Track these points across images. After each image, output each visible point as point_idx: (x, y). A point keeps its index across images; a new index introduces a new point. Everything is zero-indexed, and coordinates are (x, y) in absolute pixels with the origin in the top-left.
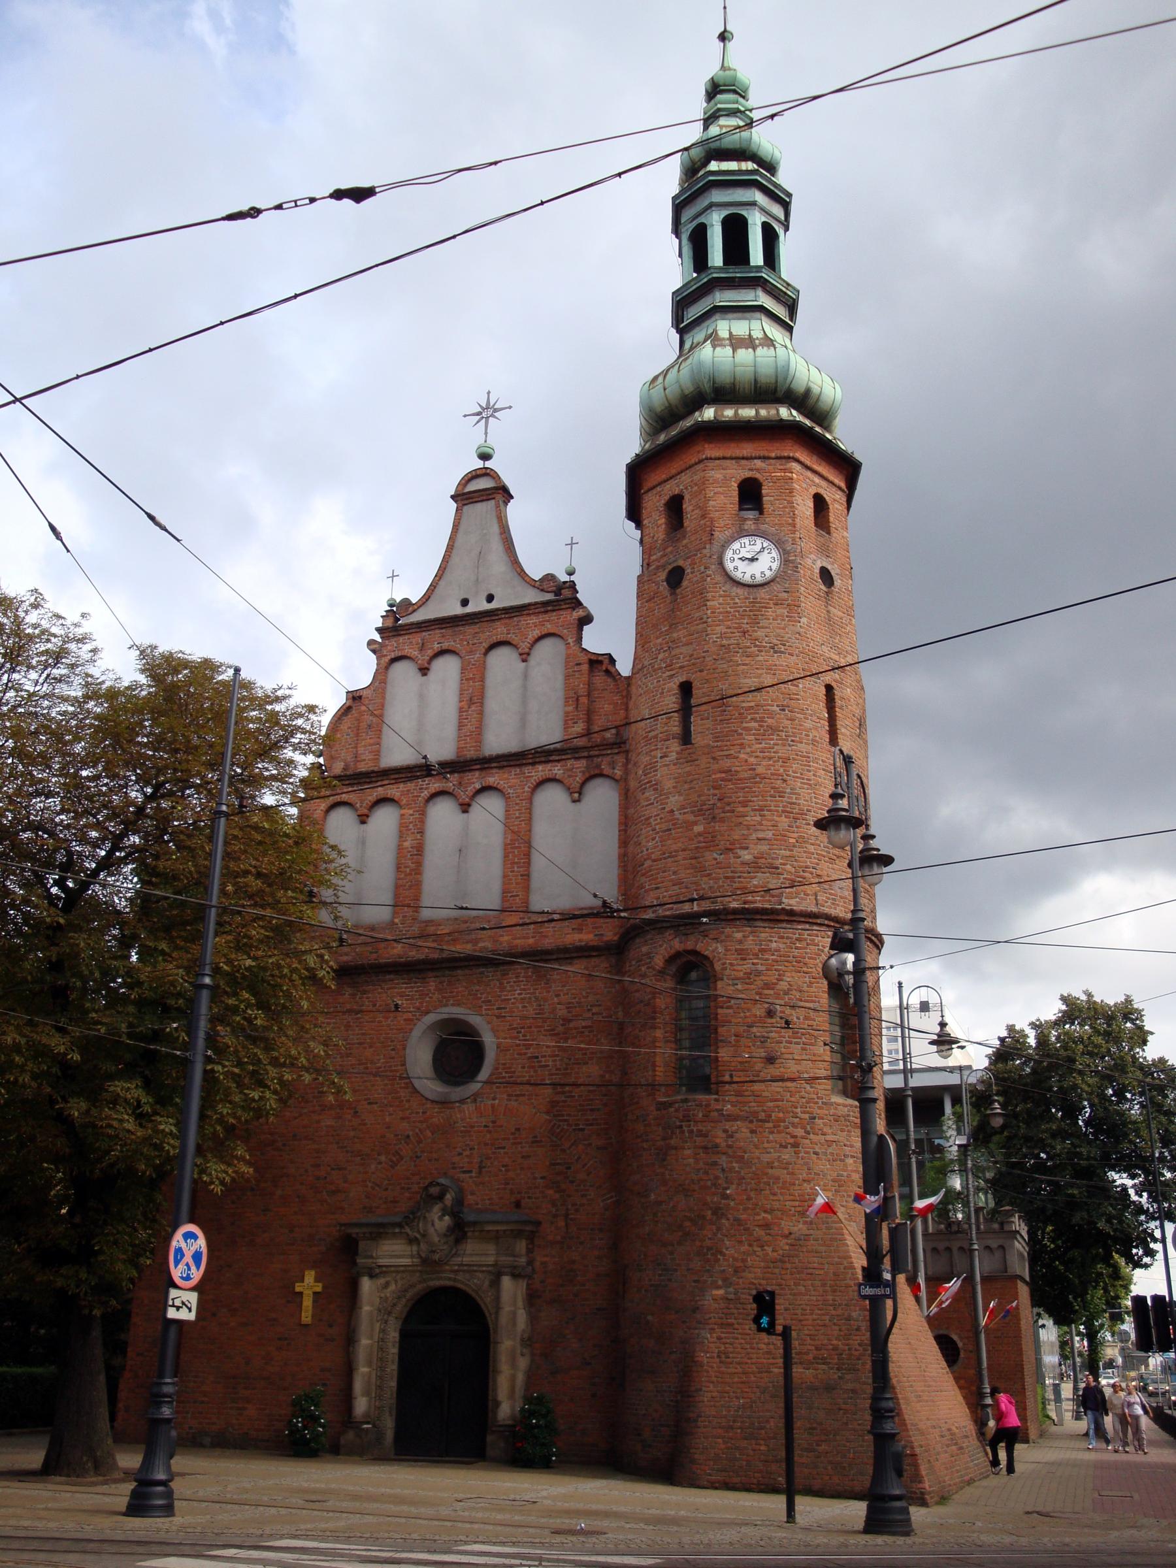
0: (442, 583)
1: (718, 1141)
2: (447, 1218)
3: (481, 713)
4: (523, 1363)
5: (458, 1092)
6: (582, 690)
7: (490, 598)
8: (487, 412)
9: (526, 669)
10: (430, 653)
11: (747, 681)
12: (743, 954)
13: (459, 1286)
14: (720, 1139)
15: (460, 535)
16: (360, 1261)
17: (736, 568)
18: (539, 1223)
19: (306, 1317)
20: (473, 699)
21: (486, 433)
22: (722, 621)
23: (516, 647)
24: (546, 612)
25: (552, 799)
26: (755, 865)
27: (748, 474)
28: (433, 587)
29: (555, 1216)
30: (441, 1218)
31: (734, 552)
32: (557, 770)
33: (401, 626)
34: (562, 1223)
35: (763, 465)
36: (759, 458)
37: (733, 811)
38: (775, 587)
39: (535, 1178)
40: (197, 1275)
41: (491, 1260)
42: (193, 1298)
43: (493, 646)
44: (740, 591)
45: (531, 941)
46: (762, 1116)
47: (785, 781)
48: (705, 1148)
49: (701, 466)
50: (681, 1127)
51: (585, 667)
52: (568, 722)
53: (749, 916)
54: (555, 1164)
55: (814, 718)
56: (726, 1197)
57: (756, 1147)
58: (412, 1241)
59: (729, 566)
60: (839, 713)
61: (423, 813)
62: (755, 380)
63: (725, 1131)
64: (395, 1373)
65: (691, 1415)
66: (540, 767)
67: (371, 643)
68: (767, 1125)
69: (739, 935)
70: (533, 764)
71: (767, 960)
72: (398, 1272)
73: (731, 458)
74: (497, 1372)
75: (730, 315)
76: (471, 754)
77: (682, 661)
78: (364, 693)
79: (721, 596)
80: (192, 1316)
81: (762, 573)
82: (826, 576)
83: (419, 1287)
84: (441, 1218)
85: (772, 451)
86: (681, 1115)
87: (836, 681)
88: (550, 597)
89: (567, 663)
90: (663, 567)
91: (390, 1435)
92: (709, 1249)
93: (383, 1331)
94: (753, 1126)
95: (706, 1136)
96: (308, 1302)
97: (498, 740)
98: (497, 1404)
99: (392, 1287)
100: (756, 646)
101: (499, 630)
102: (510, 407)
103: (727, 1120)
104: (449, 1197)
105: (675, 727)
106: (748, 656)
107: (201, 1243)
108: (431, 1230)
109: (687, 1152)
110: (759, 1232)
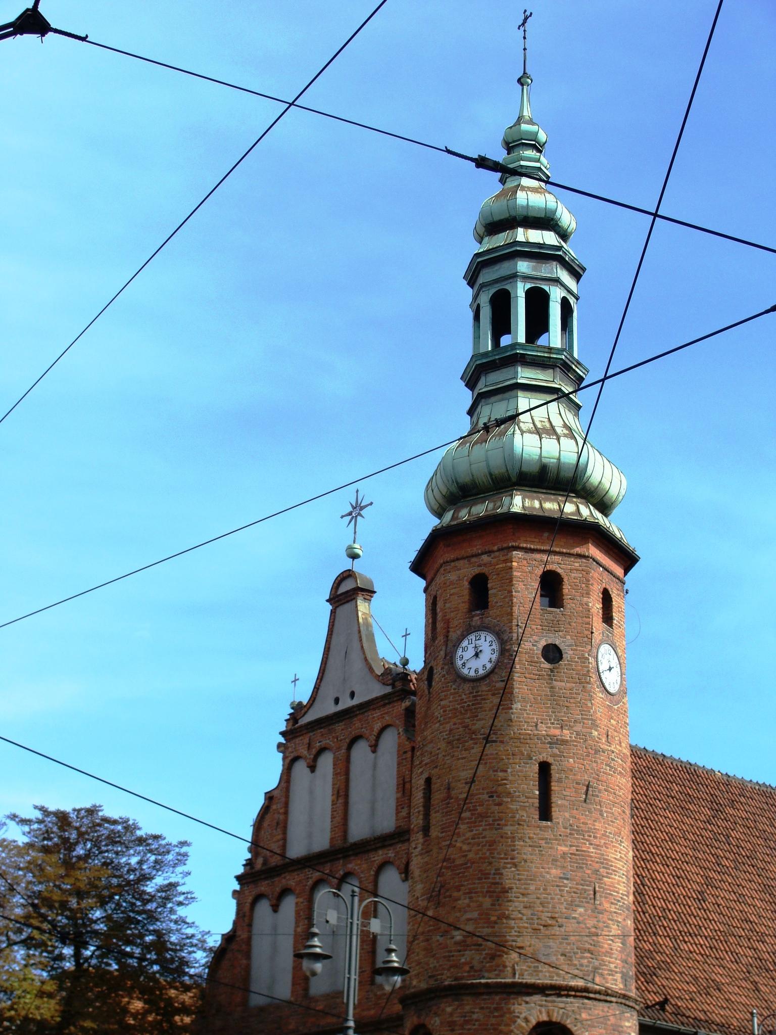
0: (323, 684)
3: (346, 804)
7: (352, 695)
8: (356, 511)
9: (375, 758)
10: (314, 751)
11: (465, 773)
15: (334, 636)
21: (355, 533)
22: (450, 718)
24: (384, 705)
26: (463, 945)
27: (477, 570)
28: (317, 689)
32: (391, 854)
33: (301, 726)
35: (489, 559)
36: (486, 553)
37: (450, 896)
38: (495, 678)
44: (467, 686)
45: (372, 1012)
47: (490, 863)
49: (442, 569)
51: (409, 754)
53: (458, 991)
55: (523, 799)
60: (554, 786)
61: (310, 901)
62: (491, 474)
66: (380, 852)
67: (279, 745)
69: (449, 1009)
70: (376, 849)
71: (469, 1029)
73: (463, 558)
75: (493, 399)
76: (339, 843)
77: (426, 760)
78: (275, 793)
79: (451, 694)
81: (484, 666)
82: (553, 654)
85: (494, 545)
87: (554, 756)
88: (389, 689)
89: (398, 751)
97: (359, 830)
100: (472, 739)
101: (357, 726)
102: (371, 504)
106: (466, 750)
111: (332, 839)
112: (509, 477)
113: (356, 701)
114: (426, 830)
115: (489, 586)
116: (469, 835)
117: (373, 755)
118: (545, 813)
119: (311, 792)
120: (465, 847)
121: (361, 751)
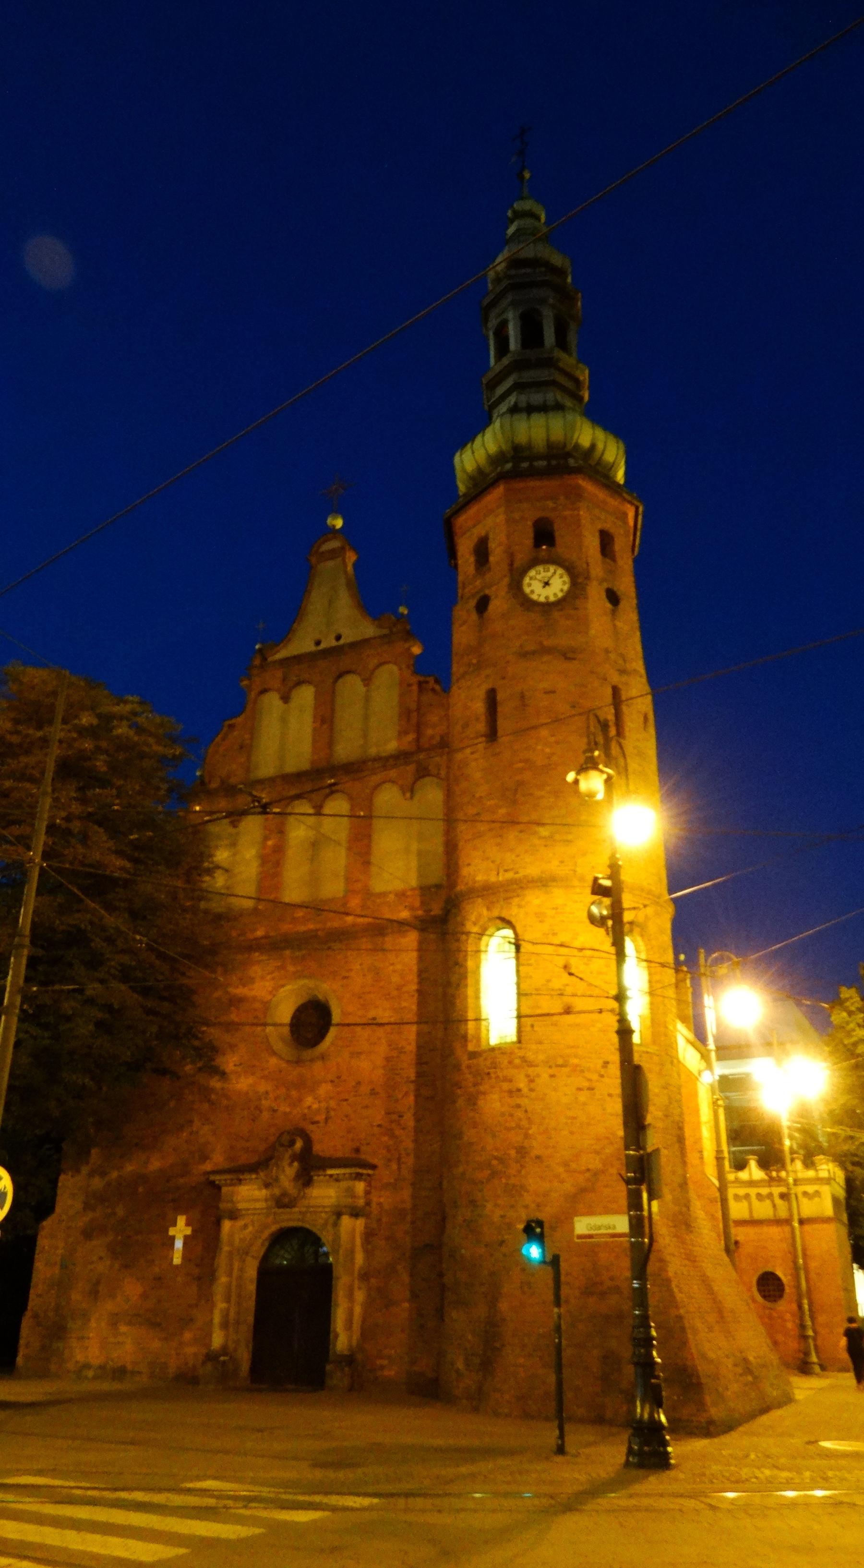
1: (522, 1085)
2: (296, 1164)
3: (331, 729)
4: (360, 1296)
5: (308, 1054)
6: (413, 706)
7: (338, 638)
9: (368, 691)
12: (541, 917)
13: (307, 1226)
14: (522, 1084)
16: (223, 1206)
17: (532, 592)
18: (374, 1167)
19: (177, 1260)
20: (326, 719)
23: (360, 674)
25: (388, 797)
29: (390, 1160)
30: (290, 1164)
31: (531, 578)
32: (393, 773)
34: (394, 1166)
39: (372, 1126)
41: (333, 1201)
43: (340, 676)
46: (560, 1061)
48: (510, 1092)
50: (489, 1074)
51: (415, 688)
52: (402, 733)
54: (389, 1114)
56: (527, 1136)
57: (555, 1090)
58: (267, 1185)
59: (527, 590)
63: (528, 1076)
64: (253, 1309)
65: (497, 1345)
68: (565, 1070)
69: (537, 902)
72: (254, 1214)
74: (337, 1305)
83: (274, 1228)
84: (290, 1164)
86: (488, 1063)
88: (385, 631)
90: (473, 596)
91: (245, 1367)
92: (514, 1186)
93: (241, 1270)
94: (552, 1071)
95: (511, 1081)
96: (179, 1244)
98: (337, 1336)
99: (250, 1228)
103: (528, 1066)
104: (299, 1144)
105: (482, 727)
108: (282, 1177)
109: (496, 1097)
110: (561, 1170)
111: (313, 762)
112: (565, 445)
113: (342, 642)
114: (492, 734)
115: (556, 527)
116: (553, 739)
117: (364, 689)
118: (620, 733)
119: (284, 720)
120: (548, 750)
121: (352, 685)
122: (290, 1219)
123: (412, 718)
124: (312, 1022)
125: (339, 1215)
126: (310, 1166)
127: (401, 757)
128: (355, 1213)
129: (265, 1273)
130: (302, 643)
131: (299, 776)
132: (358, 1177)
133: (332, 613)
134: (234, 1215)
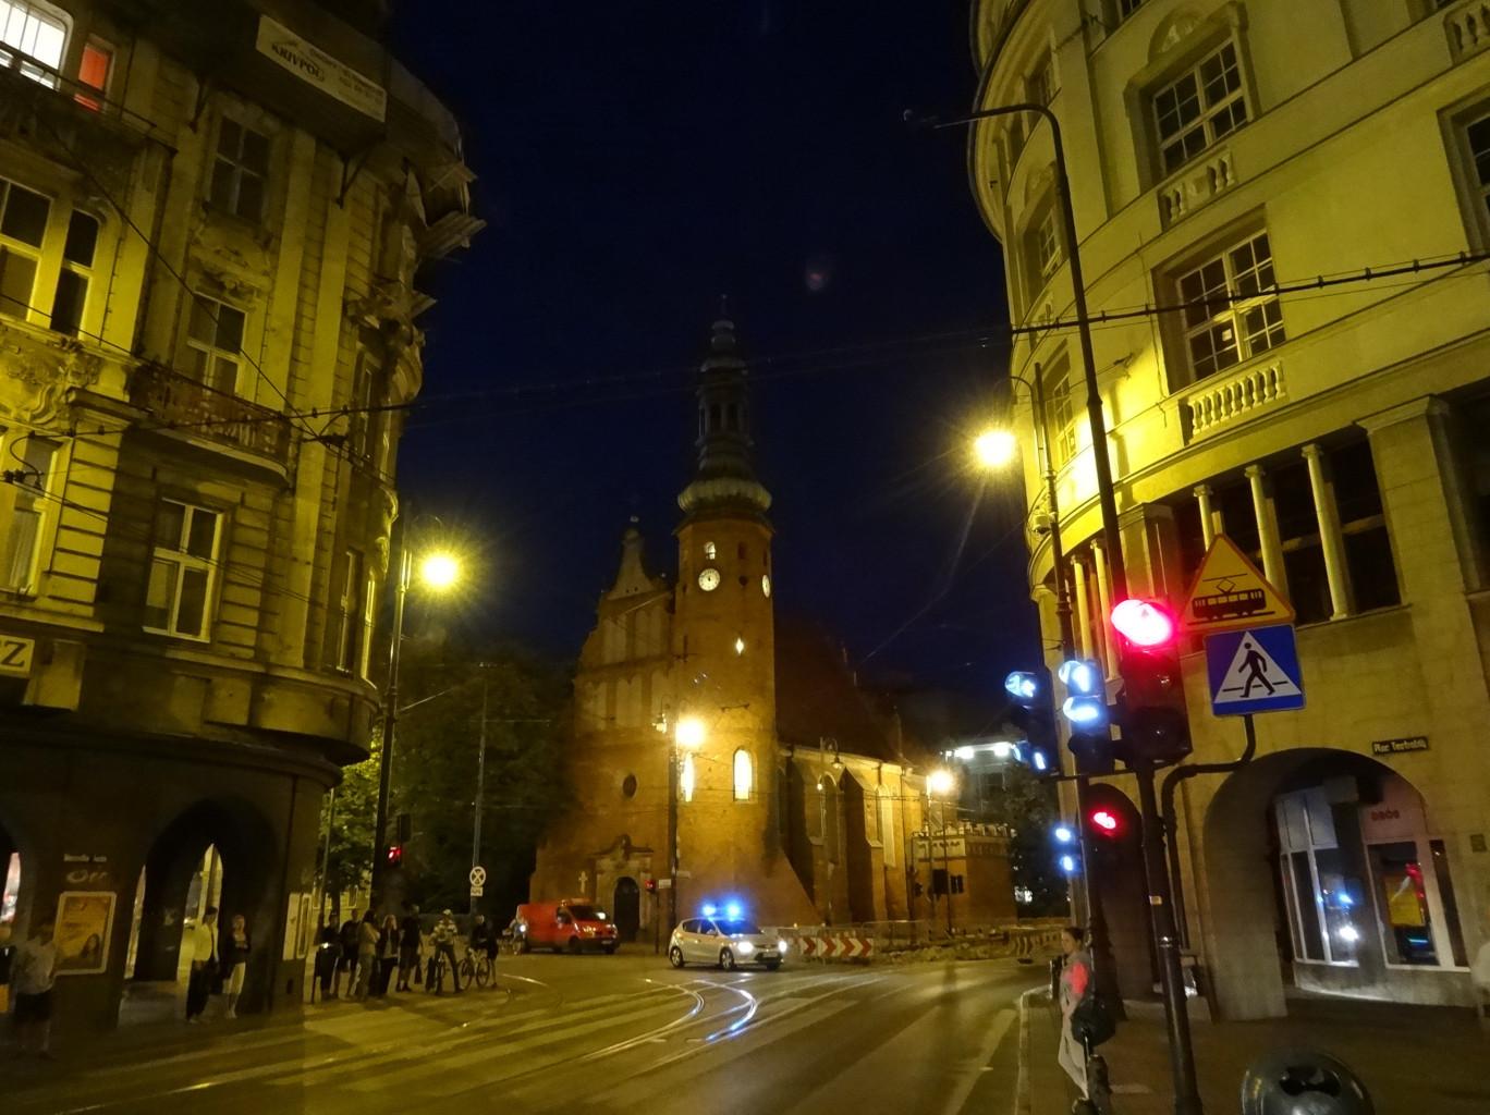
4: (649, 905)
7: (636, 589)
20: (632, 633)
40: (482, 882)
42: (481, 889)
58: (614, 859)
80: (481, 895)
96: (583, 885)
107: (483, 871)
113: (638, 592)
122: (623, 874)
123: (668, 636)
124: (630, 785)
125: (639, 872)
126: (629, 850)
127: (661, 658)
128: (646, 871)
129: (616, 896)
130: (620, 592)
131: (621, 665)
132: (647, 856)
133: (632, 578)
134: (602, 872)
